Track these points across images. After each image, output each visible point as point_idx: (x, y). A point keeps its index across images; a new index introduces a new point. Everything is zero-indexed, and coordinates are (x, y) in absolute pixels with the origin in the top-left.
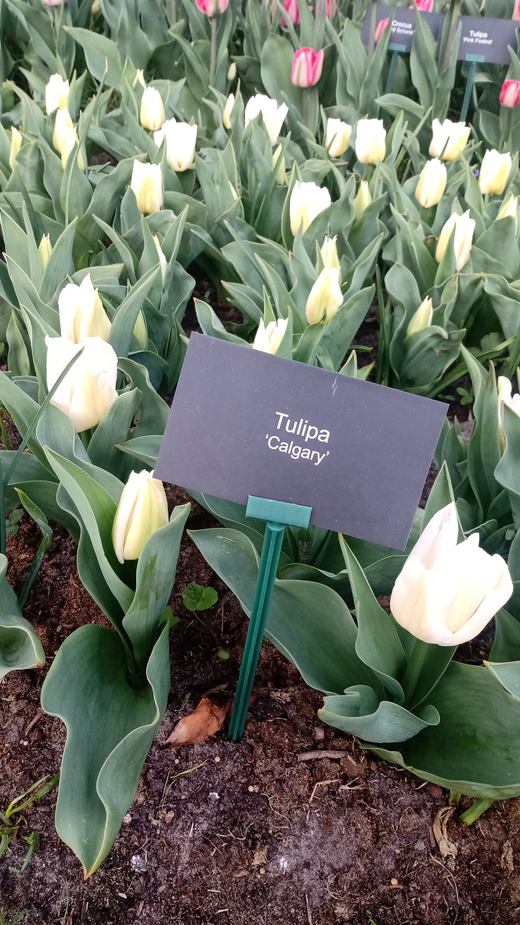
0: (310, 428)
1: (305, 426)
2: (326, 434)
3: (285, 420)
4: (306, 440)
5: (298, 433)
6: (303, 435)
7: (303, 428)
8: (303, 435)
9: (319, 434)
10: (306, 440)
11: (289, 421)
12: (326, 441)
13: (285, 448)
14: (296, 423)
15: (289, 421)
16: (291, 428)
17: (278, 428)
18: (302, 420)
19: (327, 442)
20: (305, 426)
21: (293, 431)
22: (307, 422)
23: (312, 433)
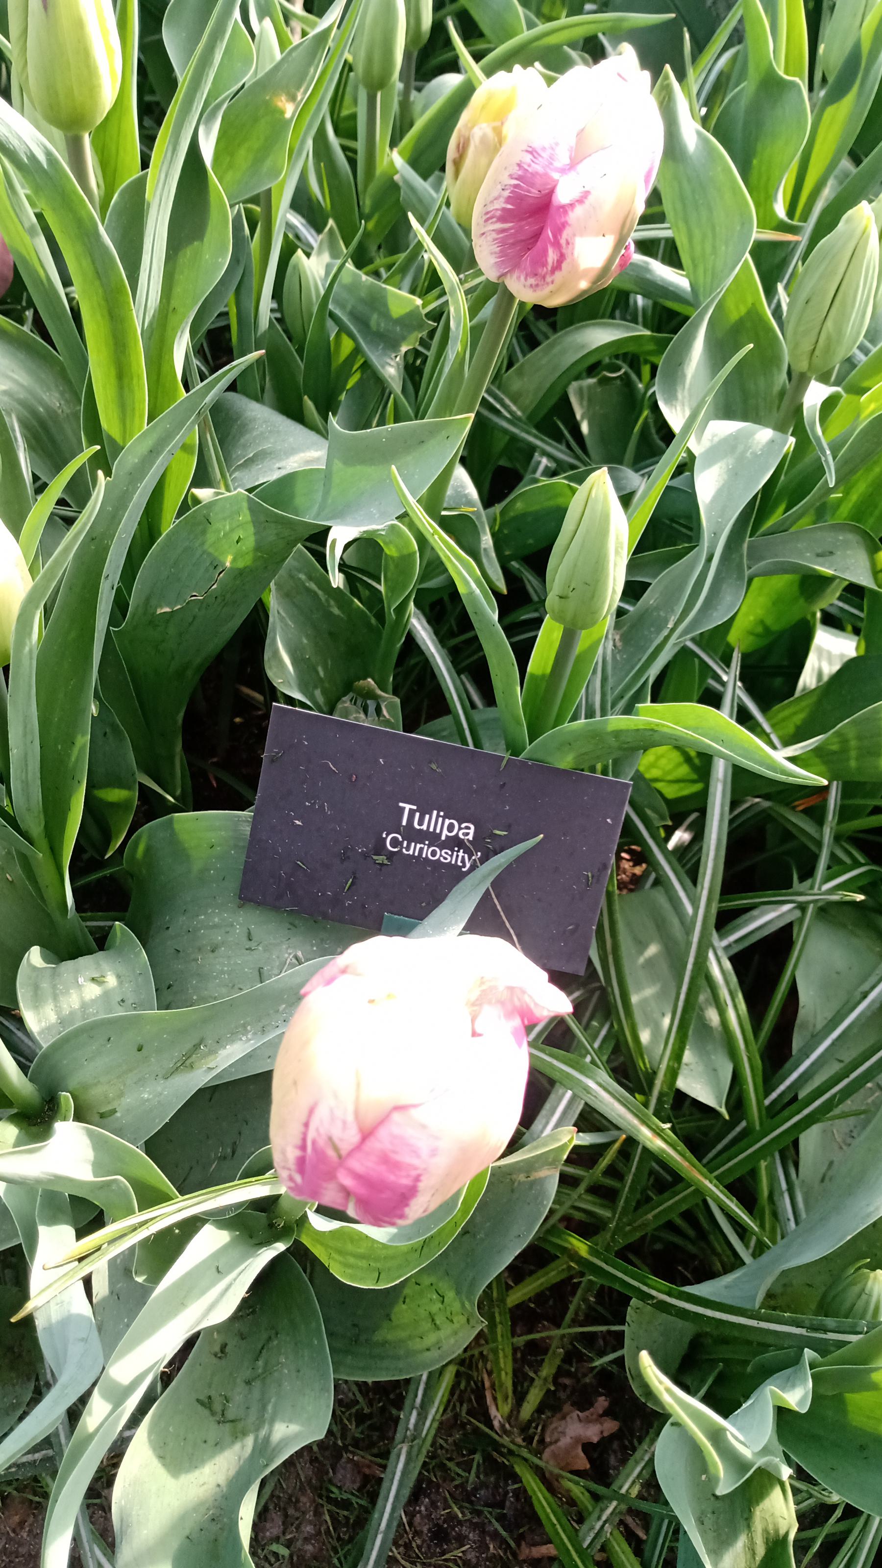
0: (447, 822)
1: (440, 819)
2: (468, 828)
3: (412, 813)
4: (443, 838)
5: (431, 830)
6: (438, 831)
7: (435, 822)
8: (438, 831)
9: (460, 829)
10: (443, 838)
11: (418, 814)
12: (470, 837)
13: (414, 849)
14: (427, 816)
15: (418, 814)
16: (421, 823)
17: (404, 823)
18: (435, 812)
19: (471, 839)
20: (440, 819)
21: (424, 827)
22: (442, 814)
23: (451, 828)
